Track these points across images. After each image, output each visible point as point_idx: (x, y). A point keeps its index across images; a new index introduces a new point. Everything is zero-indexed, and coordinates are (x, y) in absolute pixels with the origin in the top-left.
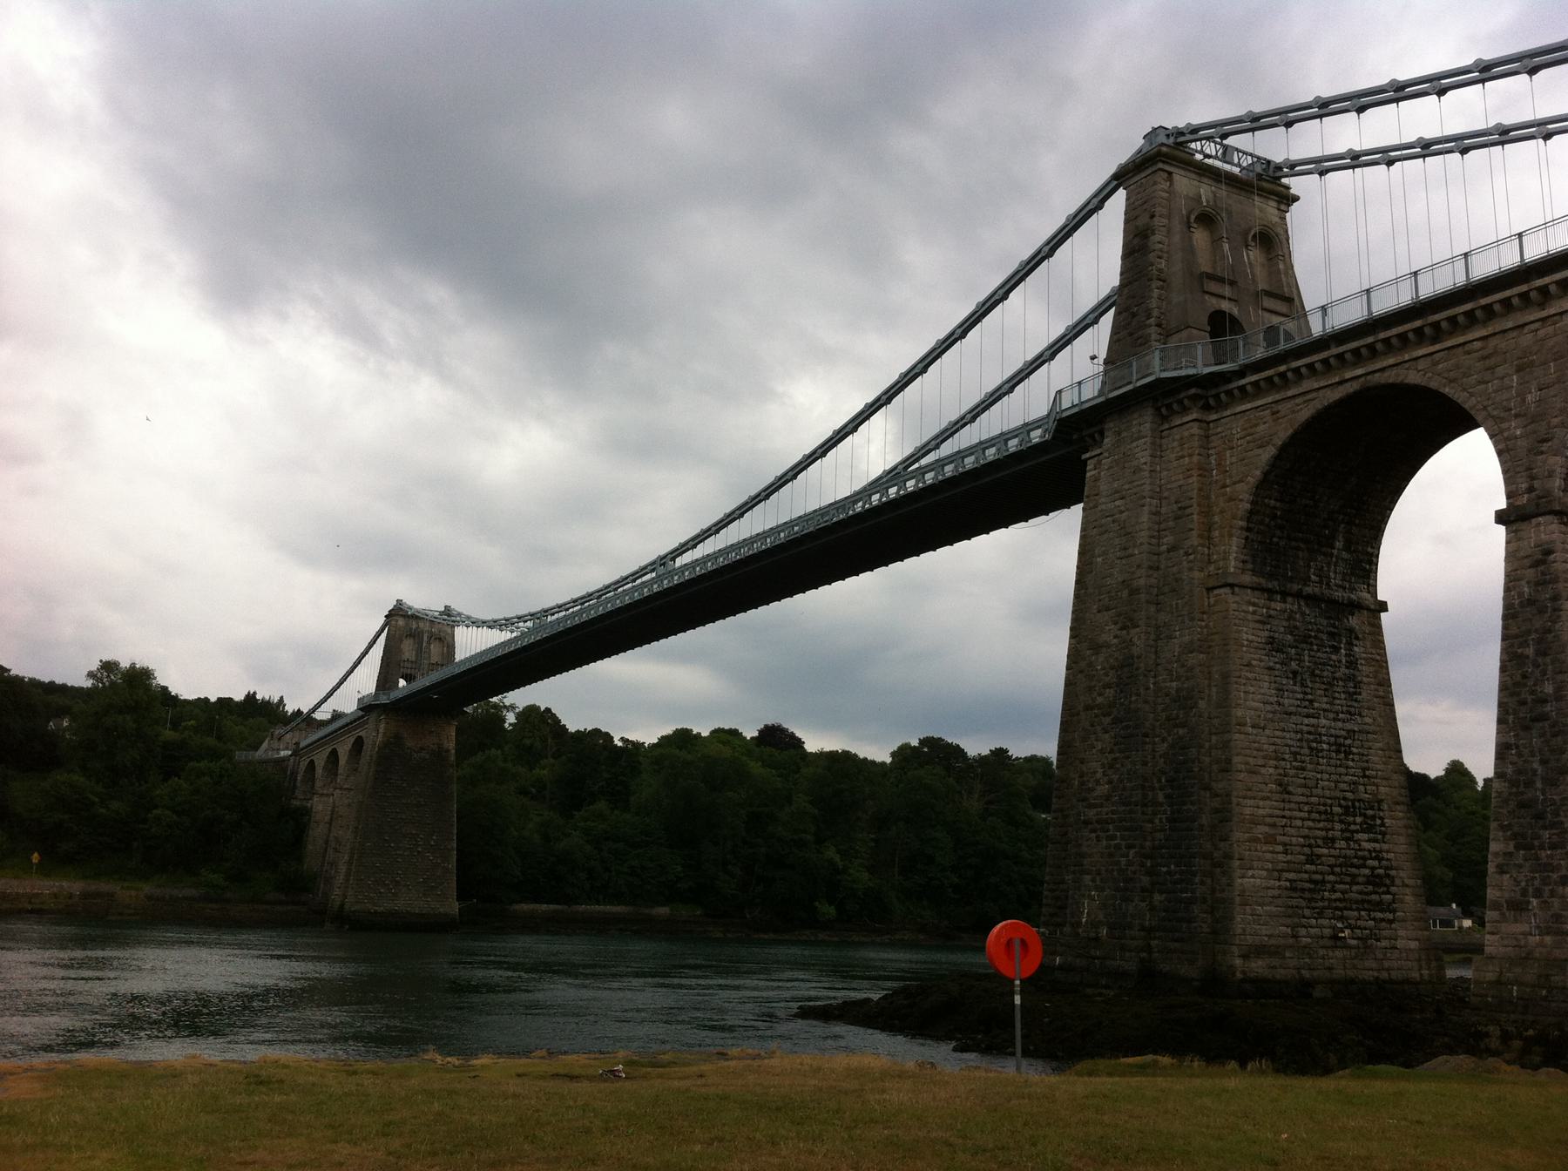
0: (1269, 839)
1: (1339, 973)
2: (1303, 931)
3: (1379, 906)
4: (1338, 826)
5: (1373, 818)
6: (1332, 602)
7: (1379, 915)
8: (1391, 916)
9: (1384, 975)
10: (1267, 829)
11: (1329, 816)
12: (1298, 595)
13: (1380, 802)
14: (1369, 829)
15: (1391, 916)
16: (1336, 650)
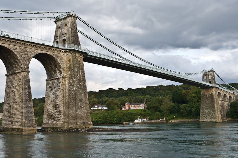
0: (47, 111)
1: (52, 126)
2: (49, 121)
3: (59, 118)
4: (55, 108)
5: (59, 106)
6: (57, 79)
7: (58, 119)
8: (60, 119)
9: (57, 126)
10: (47, 110)
11: (54, 107)
12: (53, 79)
13: (60, 104)
14: (59, 108)
15: (60, 119)
16: (57, 85)
